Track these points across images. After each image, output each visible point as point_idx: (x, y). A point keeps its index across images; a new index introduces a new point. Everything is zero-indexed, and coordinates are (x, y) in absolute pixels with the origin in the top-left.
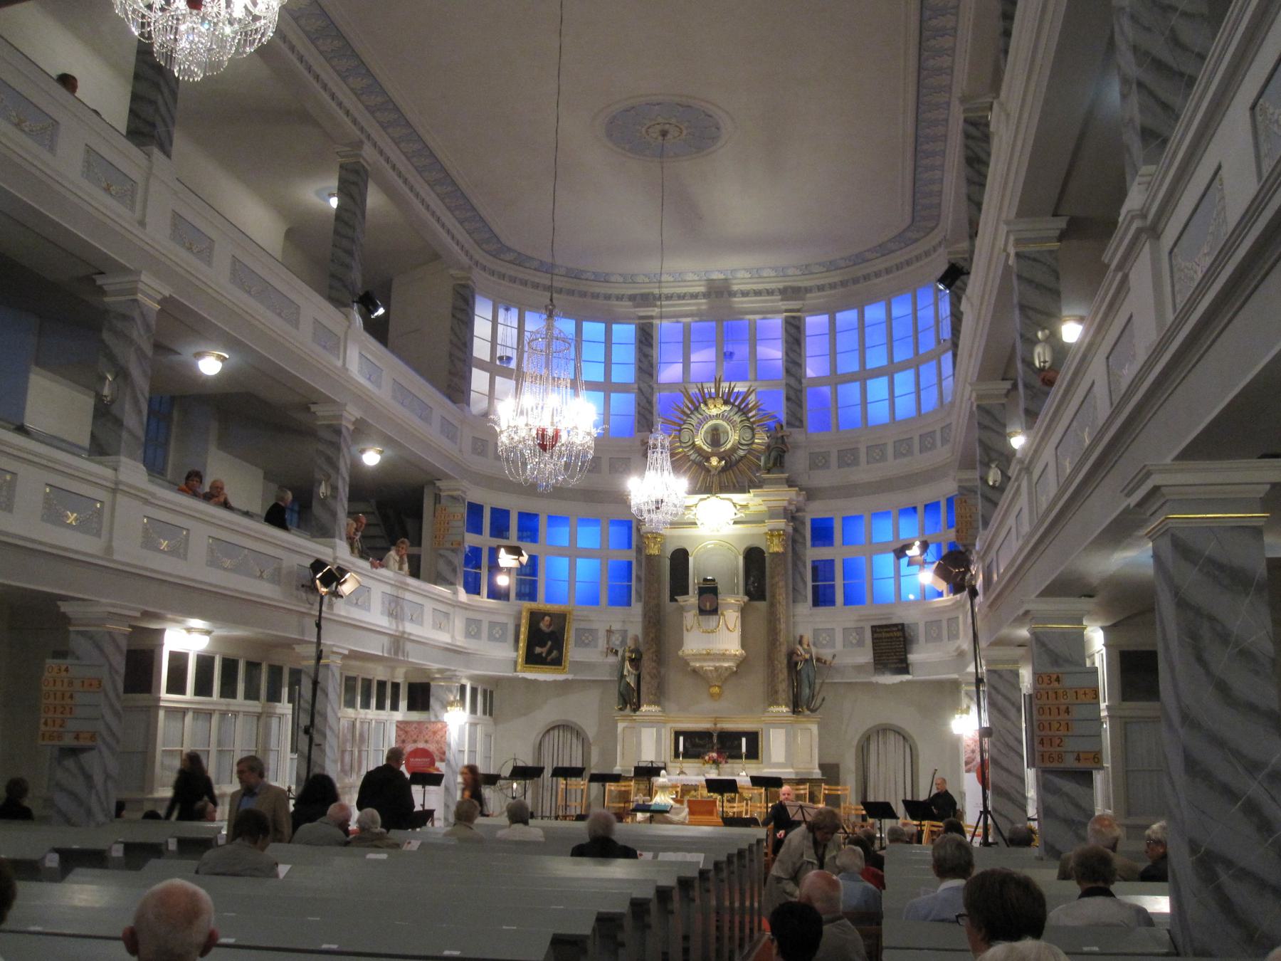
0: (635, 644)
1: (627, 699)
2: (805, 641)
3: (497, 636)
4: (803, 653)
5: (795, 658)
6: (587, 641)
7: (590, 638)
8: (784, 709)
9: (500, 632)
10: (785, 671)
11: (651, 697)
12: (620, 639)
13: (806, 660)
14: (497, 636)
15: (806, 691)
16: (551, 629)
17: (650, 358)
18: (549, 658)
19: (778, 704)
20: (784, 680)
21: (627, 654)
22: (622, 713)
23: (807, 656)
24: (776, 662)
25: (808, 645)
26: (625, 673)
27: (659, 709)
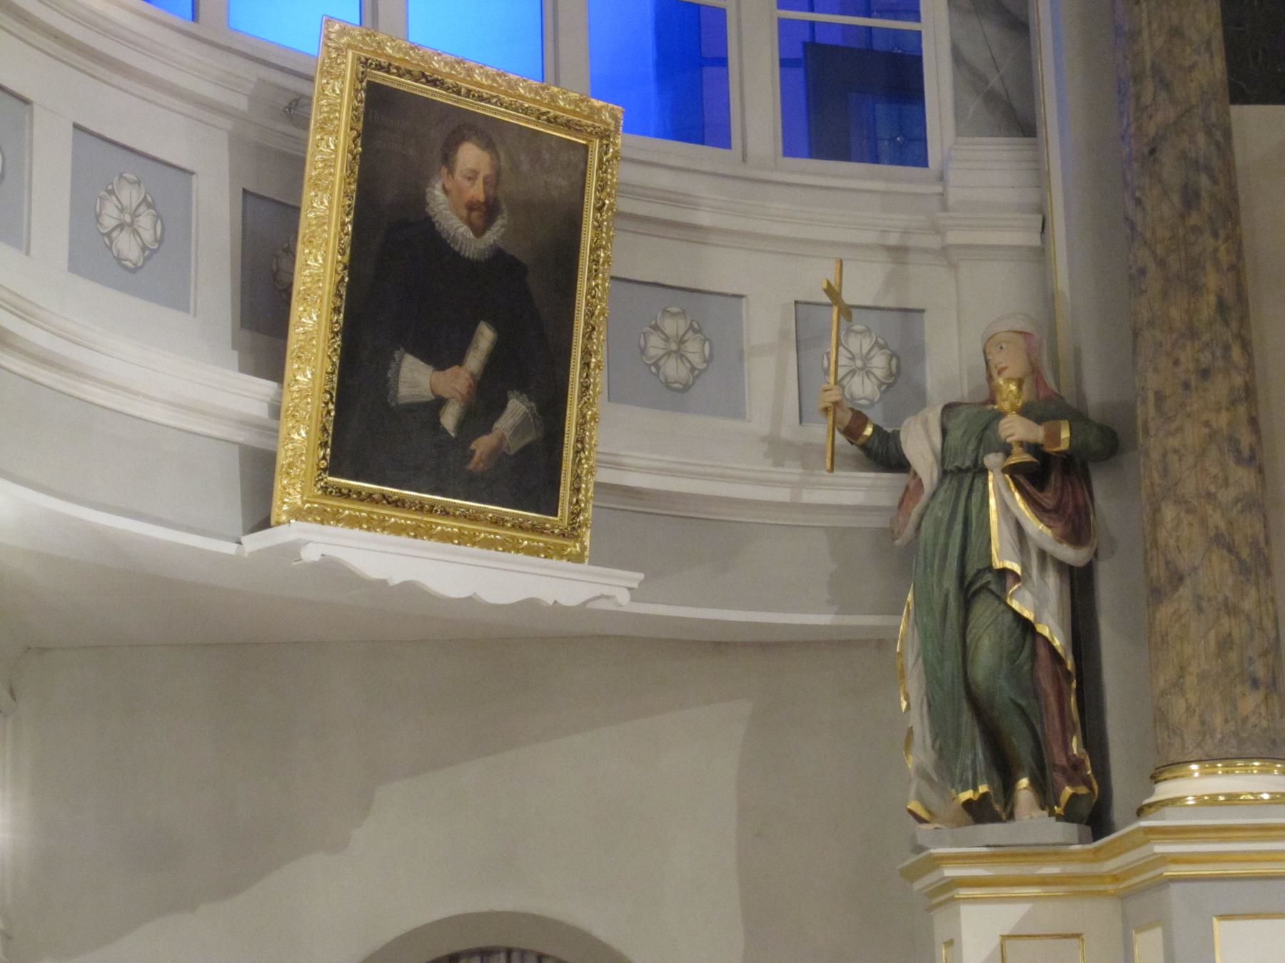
1: (1022, 747)
3: (128, 247)
6: (673, 369)
7: (694, 349)
9: (145, 222)
11: (1250, 702)
12: (879, 363)
14: (128, 247)
16: (492, 236)
18: (482, 445)
22: (992, 832)
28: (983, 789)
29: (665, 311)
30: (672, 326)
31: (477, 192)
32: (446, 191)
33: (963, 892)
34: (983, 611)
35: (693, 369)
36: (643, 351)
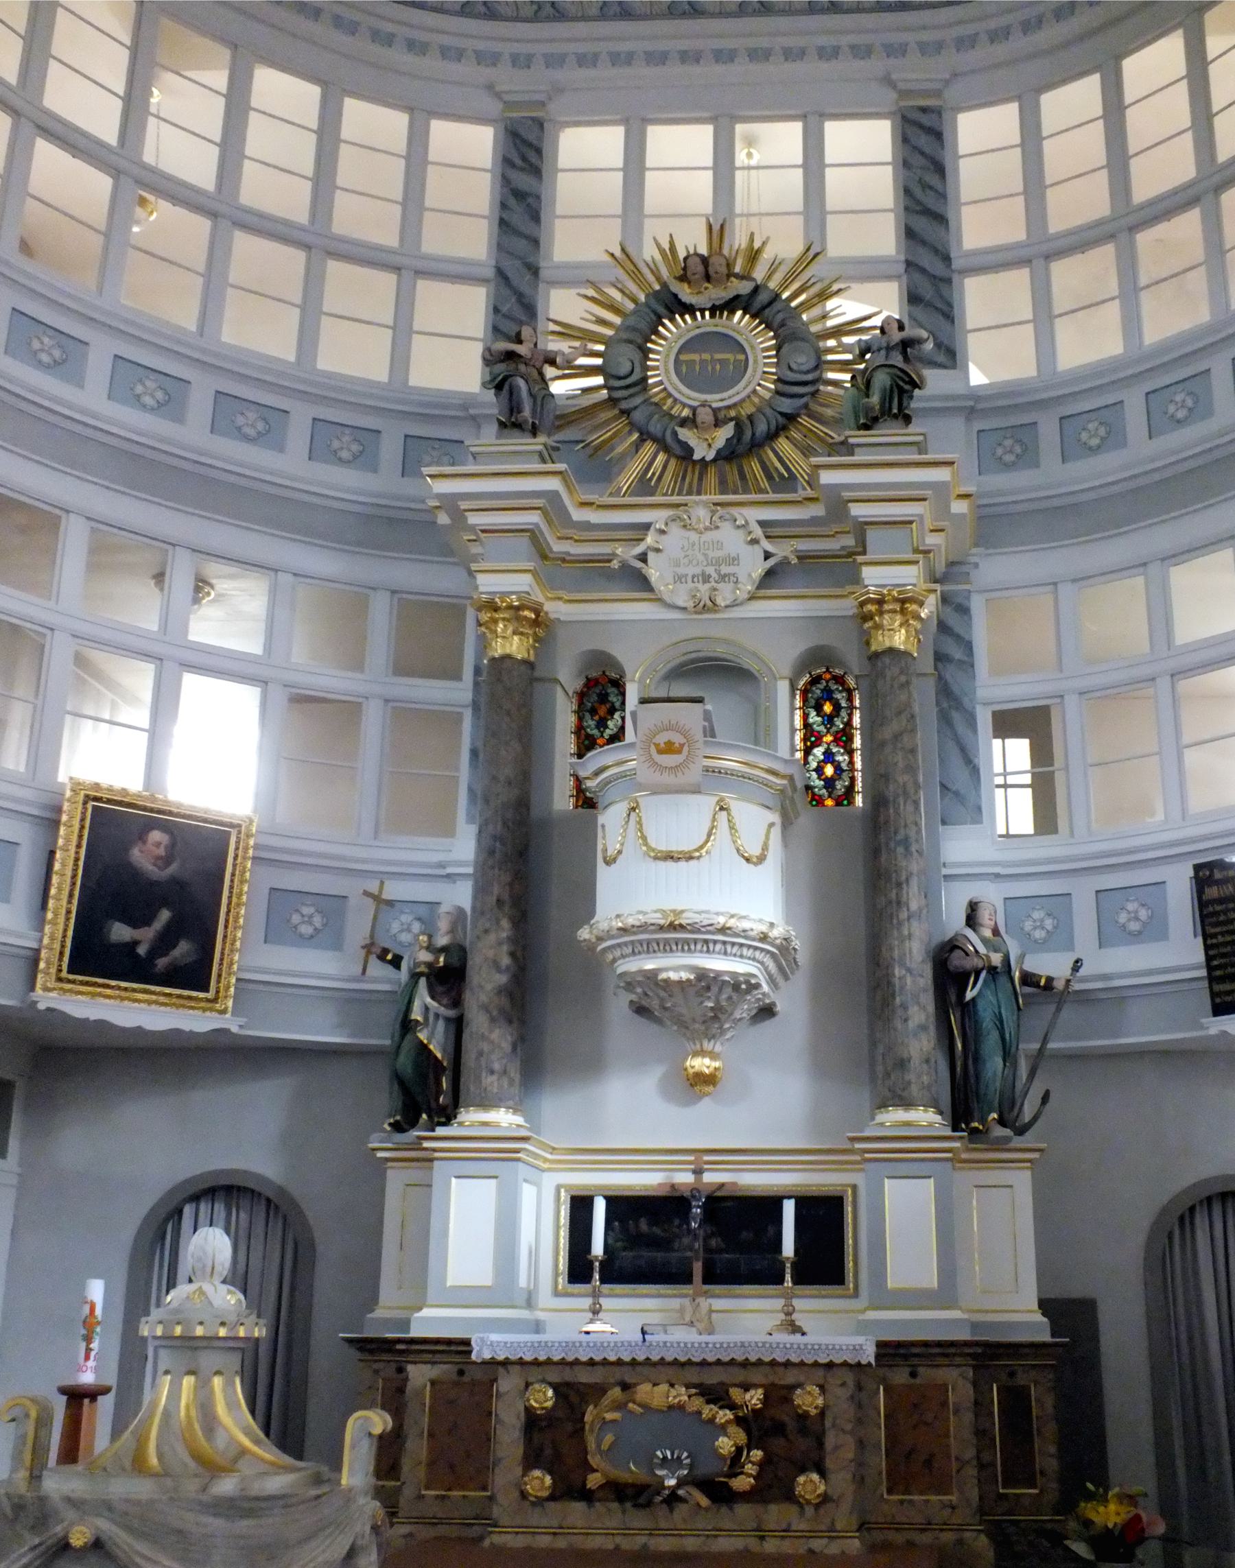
0: (452, 931)
2: (985, 916)
4: (982, 949)
5: (957, 961)
8: (926, 1118)
10: (928, 1000)
13: (992, 970)
15: (994, 1065)
17: (530, 200)
19: (907, 1103)
20: (923, 1028)
21: (425, 956)
22: (400, 1138)
23: (996, 959)
24: (898, 972)
25: (996, 932)
26: (416, 1015)
27: (519, 1120)
28: (398, 1118)
29: (303, 904)
30: (307, 910)
31: (161, 851)
32: (141, 852)
33: (390, 1164)
34: (409, 1037)
35: (316, 929)
36: (288, 921)
